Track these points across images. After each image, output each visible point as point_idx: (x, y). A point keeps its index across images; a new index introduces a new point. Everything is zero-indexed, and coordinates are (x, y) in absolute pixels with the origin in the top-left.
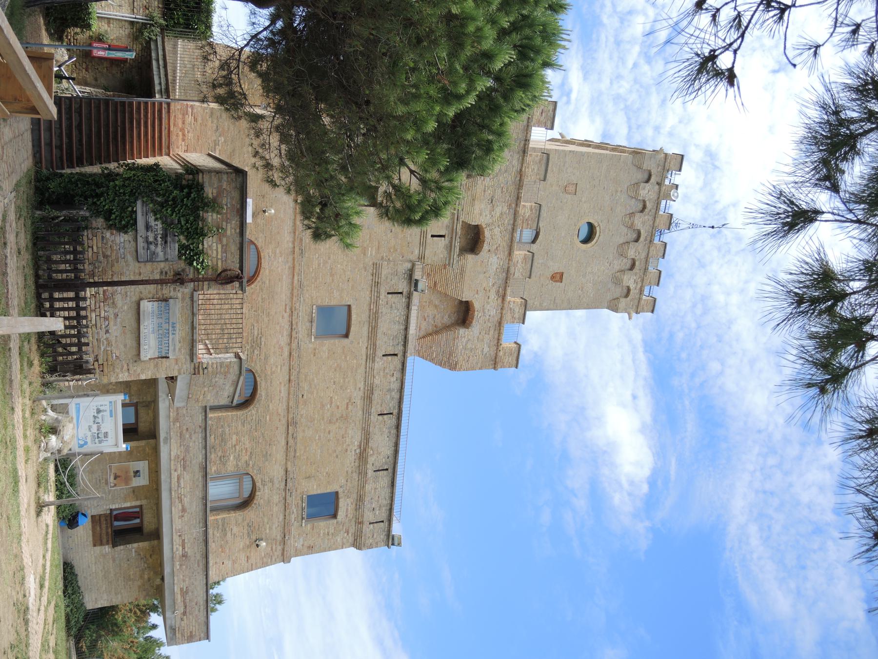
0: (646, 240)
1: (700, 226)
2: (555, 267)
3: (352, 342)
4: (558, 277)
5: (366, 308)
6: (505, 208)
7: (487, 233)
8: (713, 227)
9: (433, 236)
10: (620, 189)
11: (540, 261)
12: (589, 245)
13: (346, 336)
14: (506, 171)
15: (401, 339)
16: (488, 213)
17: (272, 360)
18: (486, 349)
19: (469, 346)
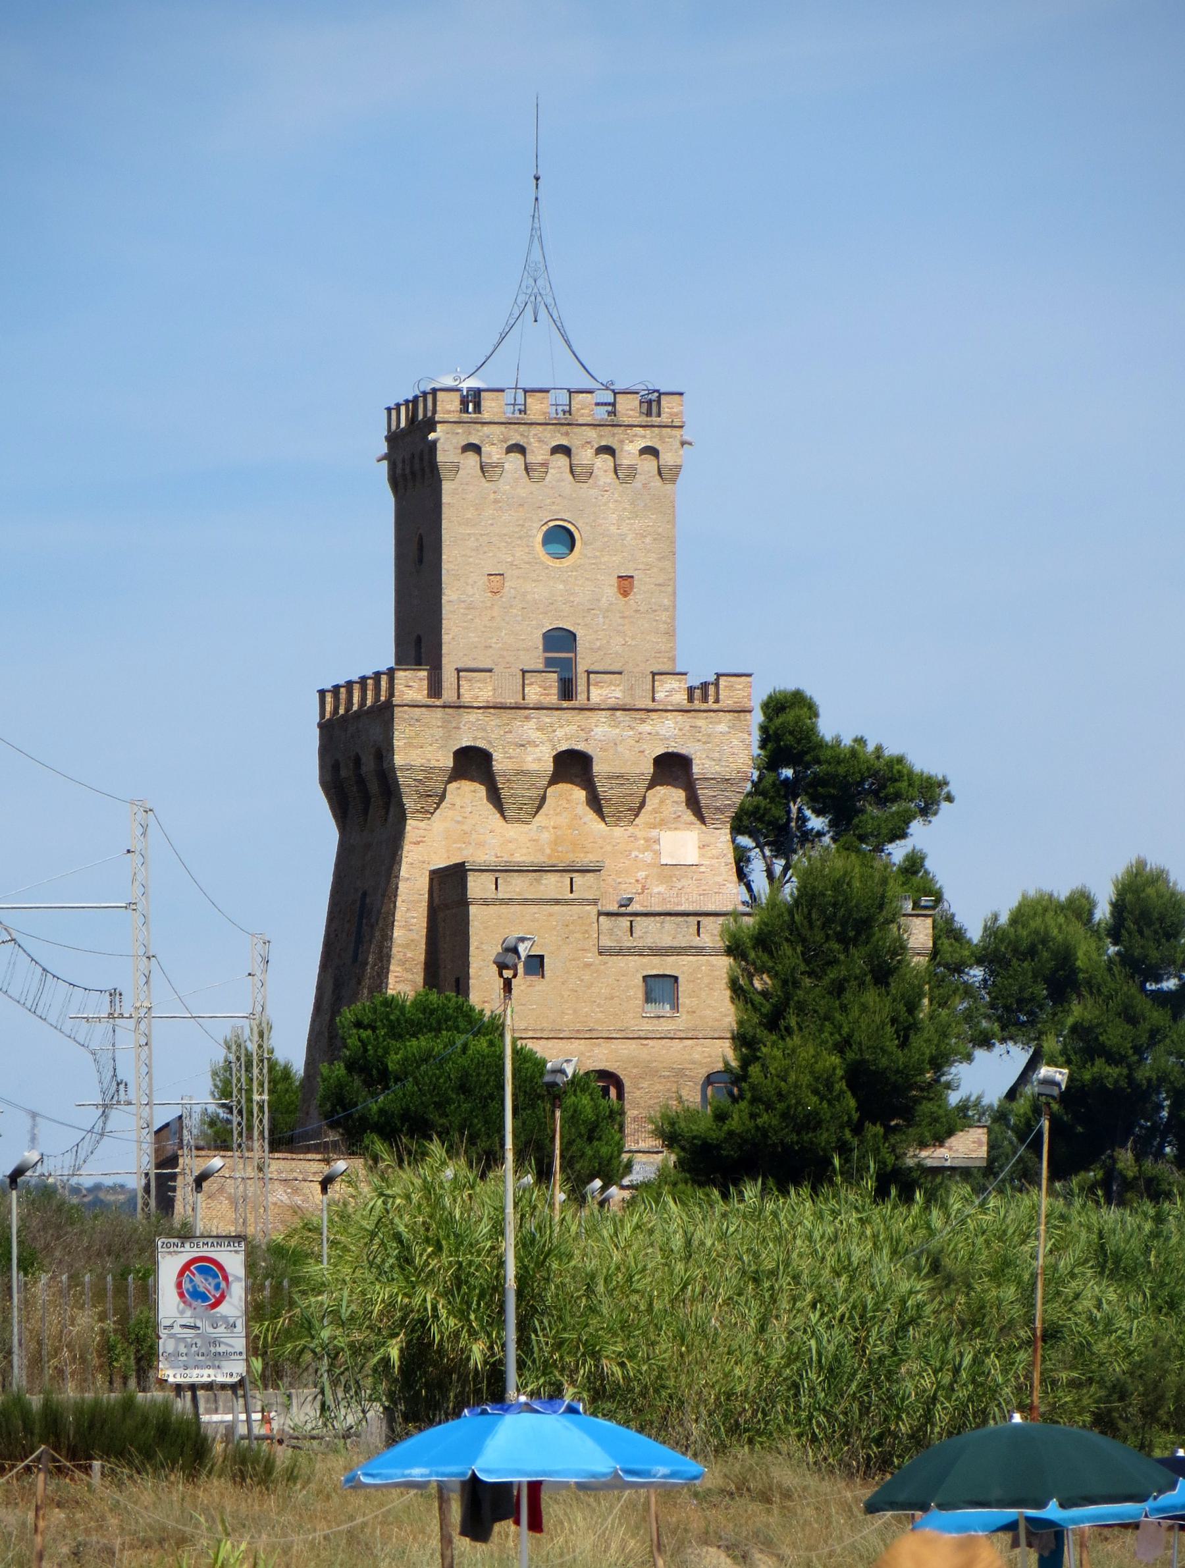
0: (567, 434)
1: (536, 208)
2: (610, 590)
3: (683, 973)
4: (625, 583)
5: (645, 960)
6: (532, 724)
7: (564, 747)
8: (537, 179)
9: (572, 891)
10: (492, 496)
11: (601, 620)
12: (578, 544)
13: (676, 978)
14: (485, 730)
15: (680, 919)
16: (537, 750)
17: (697, 1056)
18: (722, 727)
19: (717, 755)
